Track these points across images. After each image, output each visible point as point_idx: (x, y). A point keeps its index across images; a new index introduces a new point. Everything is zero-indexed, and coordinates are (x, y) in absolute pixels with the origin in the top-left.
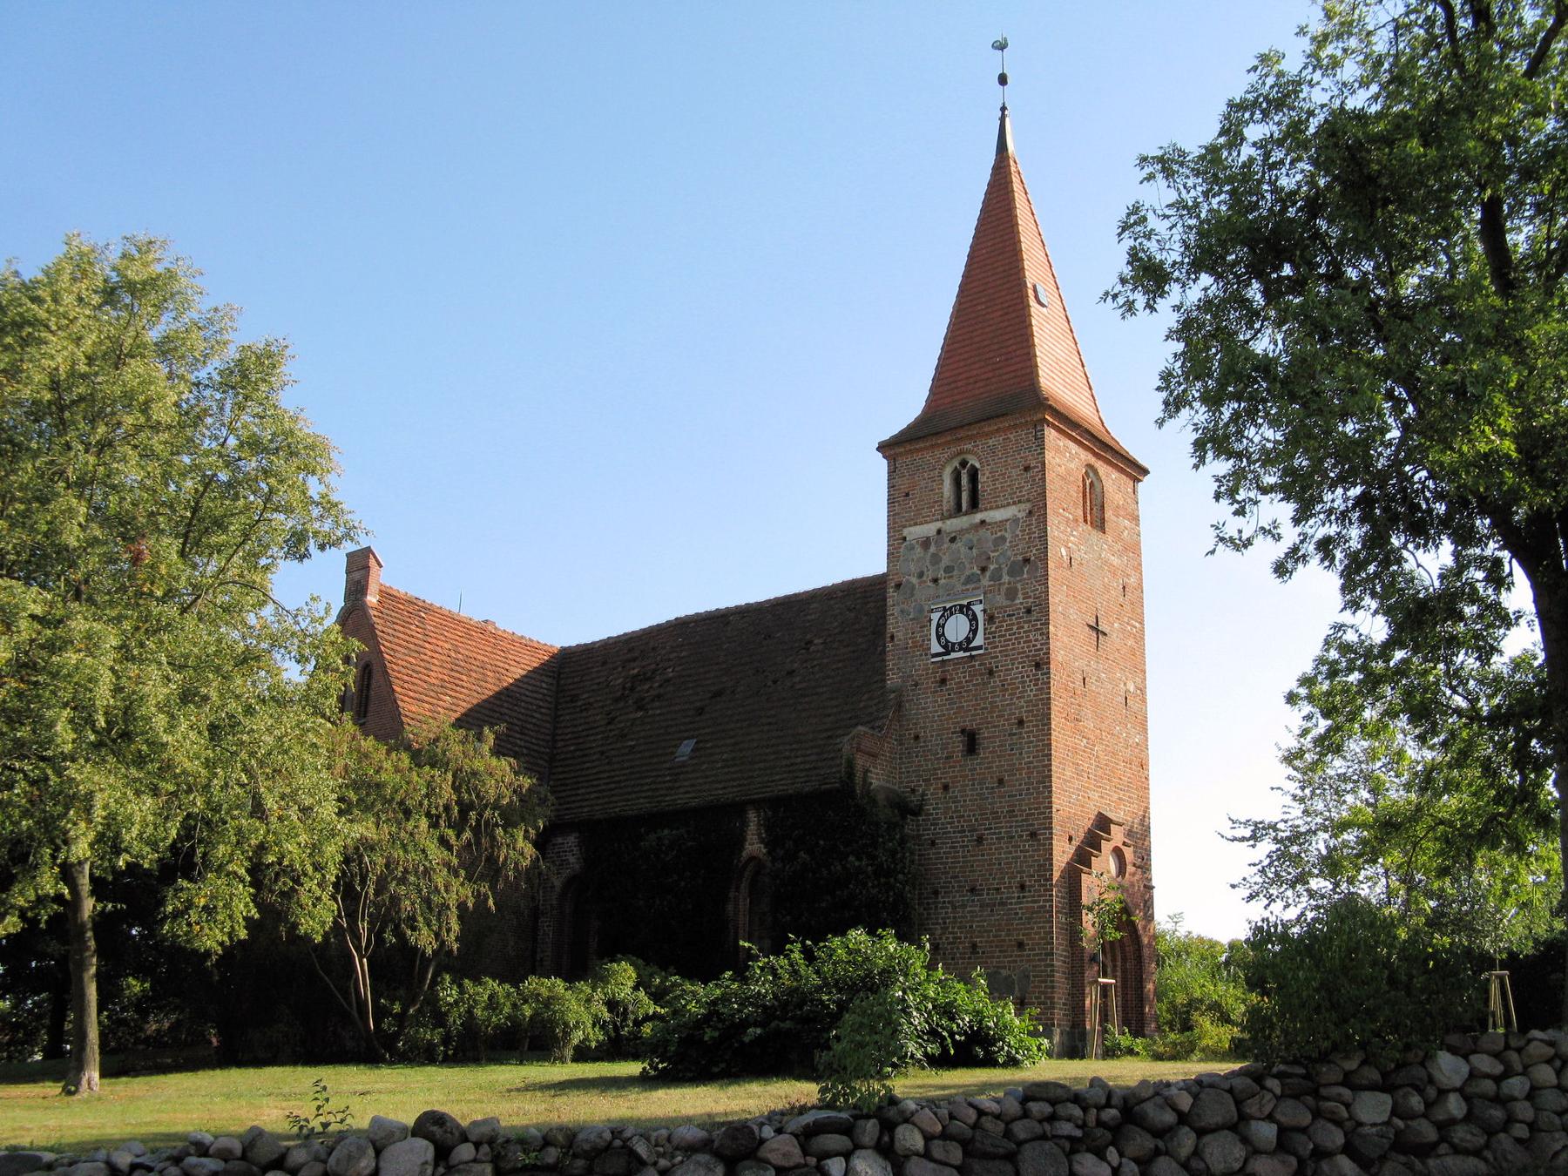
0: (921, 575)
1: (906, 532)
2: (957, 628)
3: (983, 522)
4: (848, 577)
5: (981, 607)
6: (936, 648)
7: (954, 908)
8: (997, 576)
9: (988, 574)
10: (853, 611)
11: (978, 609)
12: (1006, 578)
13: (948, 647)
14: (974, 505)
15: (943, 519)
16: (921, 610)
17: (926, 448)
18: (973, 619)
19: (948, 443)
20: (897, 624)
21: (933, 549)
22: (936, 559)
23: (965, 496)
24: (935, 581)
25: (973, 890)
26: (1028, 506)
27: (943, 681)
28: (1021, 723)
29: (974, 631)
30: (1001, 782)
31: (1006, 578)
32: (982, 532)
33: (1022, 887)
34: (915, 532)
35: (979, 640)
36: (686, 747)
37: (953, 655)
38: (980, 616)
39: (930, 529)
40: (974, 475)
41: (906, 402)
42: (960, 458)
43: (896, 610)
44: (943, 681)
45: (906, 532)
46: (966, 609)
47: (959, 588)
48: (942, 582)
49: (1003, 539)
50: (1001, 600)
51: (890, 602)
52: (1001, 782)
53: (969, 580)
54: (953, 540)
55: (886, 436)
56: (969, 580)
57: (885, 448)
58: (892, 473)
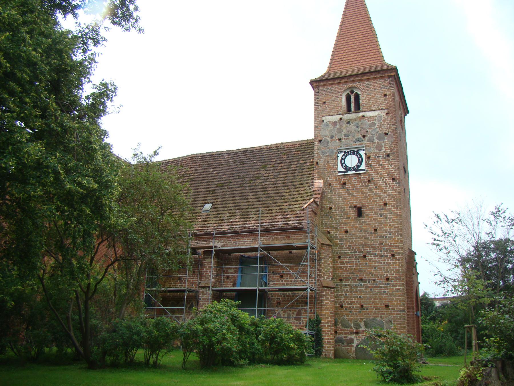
0: (332, 137)
1: (323, 118)
2: (352, 161)
3: (363, 116)
4: (279, 141)
5: (364, 152)
6: (340, 168)
7: (351, 288)
8: (371, 140)
9: (367, 138)
10: (305, 149)
11: (362, 153)
12: (376, 141)
13: (347, 169)
14: (358, 108)
15: (343, 114)
16: (332, 152)
17: (334, 84)
18: (360, 157)
19: (345, 82)
20: (319, 157)
21: (338, 126)
22: (340, 131)
23: (353, 105)
24: (340, 140)
25: (361, 280)
26: (386, 111)
27: (344, 184)
28: (385, 204)
29: (361, 163)
30: (375, 230)
31: (376, 141)
32: (363, 120)
33: (387, 279)
34: (328, 119)
35: (363, 166)
36: (208, 207)
37: (350, 173)
38: (364, 157)
39: (337, 118)
40: (357, 97)
41: (320, 68)
42: (350, 90)
43: (319, 152)
44: (344, 184)
45: (323, 118)
46: (356, 152)
47: (352, 143)
48: (343, 140)
49: (375, 124)
50: (374, 150)
51: (316, 148)
52: (375, 230)
53: (357, 140)
54: (348, 123)
55: (313, 78)
56: (357, 140)
57: (312, 82)
58: (316, 94)
